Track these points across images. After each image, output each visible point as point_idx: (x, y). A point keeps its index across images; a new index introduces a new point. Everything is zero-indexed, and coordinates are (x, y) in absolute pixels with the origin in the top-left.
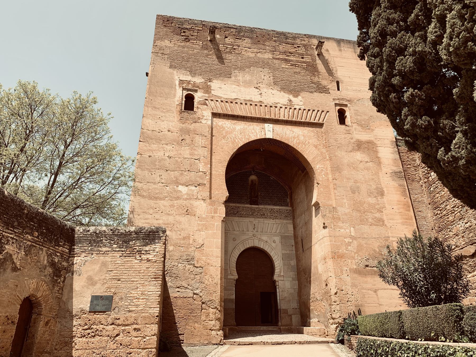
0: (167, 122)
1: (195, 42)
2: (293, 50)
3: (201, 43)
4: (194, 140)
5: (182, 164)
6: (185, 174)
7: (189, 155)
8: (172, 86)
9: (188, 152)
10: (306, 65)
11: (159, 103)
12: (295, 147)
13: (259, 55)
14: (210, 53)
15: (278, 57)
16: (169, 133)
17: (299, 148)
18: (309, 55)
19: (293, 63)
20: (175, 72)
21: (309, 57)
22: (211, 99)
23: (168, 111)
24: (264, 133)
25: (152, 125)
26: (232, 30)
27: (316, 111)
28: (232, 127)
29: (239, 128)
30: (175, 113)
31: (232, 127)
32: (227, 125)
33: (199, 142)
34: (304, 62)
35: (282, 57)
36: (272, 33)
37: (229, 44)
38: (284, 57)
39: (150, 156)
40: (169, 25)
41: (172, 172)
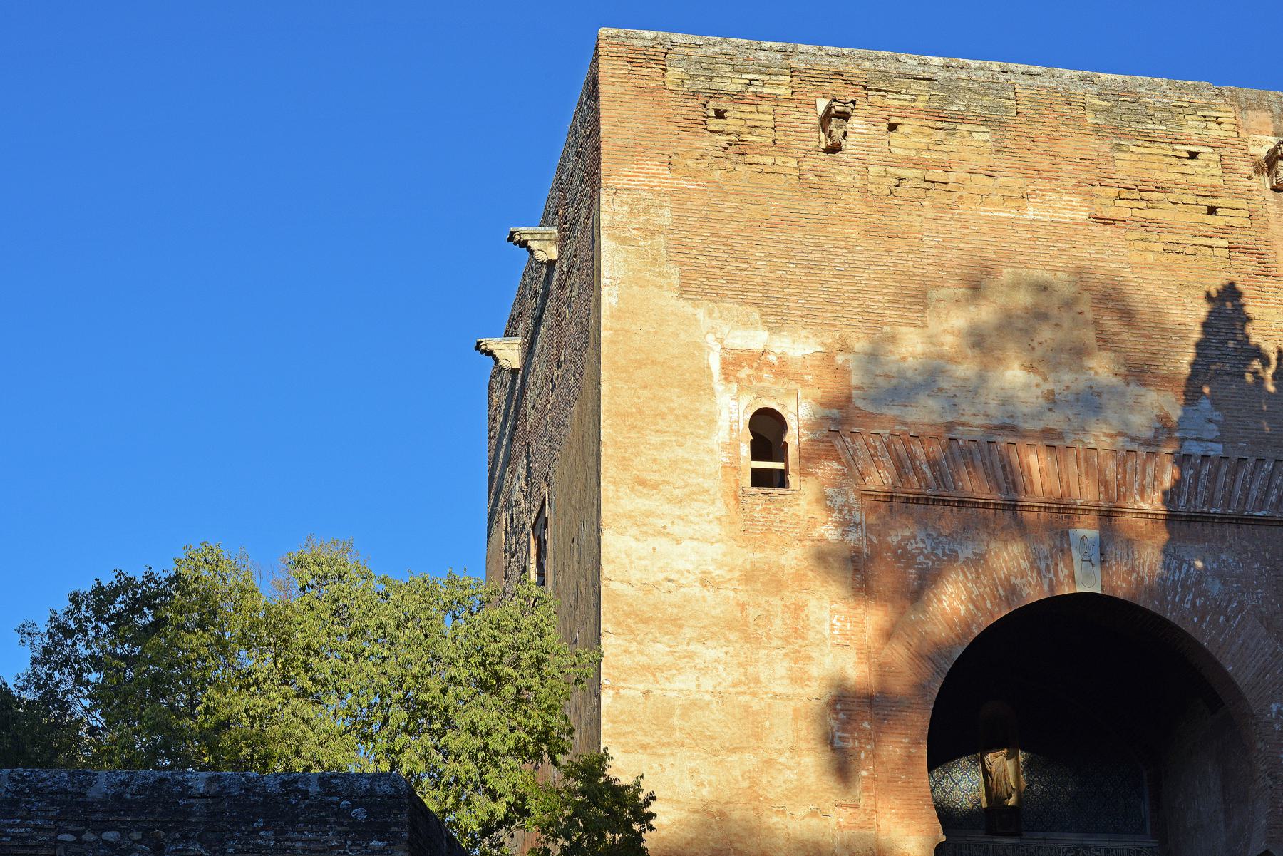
0: (695, 543)
1: (769, 161)
2: (1171, 174)
3: (793, 163)
4: (803, 615)
5: (767, 724)
6: (783, 760)
7: (786, 682)
8: (698, 385)
9: (782, 668)
10: (1225, 243)
11: (655, 461)
12: (1188, 629)
13: (1032, 212)
14: (834, 210)
15: (1110, 213)
16: (709, 594)
17: (1205, 634)
18: (1236, 195)
19: (1169, 238)
20: (700, 313)
21: (1240, 203)
22: (855, 429)
23: (691, 495)
24: (1067, 572)
25: (640, 558)
26: (915, 85)
27: (1268, 466)
28: (939, 552)
29: (971, 555)
30: (720, 504)
31: (939, 552)
32: (921, 545)
33: (820, 622)
34: (1221, 232)
35: (1126, 214)
36: (1080, 91)
37: (904, 162)
38: (1136, 212)
39: (646, 693)
40: (653, 84)
41: (734, 758)
